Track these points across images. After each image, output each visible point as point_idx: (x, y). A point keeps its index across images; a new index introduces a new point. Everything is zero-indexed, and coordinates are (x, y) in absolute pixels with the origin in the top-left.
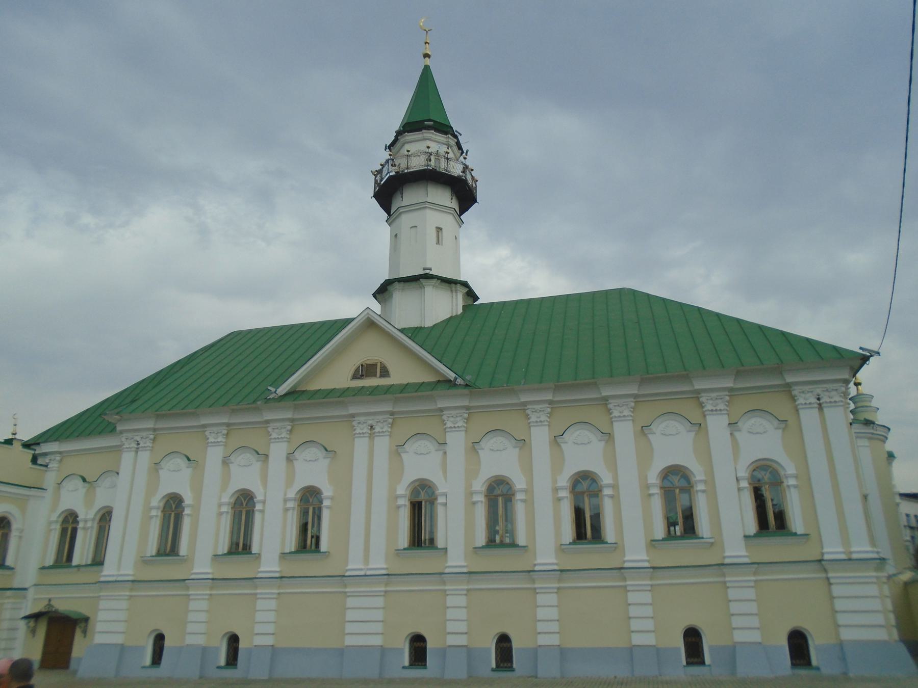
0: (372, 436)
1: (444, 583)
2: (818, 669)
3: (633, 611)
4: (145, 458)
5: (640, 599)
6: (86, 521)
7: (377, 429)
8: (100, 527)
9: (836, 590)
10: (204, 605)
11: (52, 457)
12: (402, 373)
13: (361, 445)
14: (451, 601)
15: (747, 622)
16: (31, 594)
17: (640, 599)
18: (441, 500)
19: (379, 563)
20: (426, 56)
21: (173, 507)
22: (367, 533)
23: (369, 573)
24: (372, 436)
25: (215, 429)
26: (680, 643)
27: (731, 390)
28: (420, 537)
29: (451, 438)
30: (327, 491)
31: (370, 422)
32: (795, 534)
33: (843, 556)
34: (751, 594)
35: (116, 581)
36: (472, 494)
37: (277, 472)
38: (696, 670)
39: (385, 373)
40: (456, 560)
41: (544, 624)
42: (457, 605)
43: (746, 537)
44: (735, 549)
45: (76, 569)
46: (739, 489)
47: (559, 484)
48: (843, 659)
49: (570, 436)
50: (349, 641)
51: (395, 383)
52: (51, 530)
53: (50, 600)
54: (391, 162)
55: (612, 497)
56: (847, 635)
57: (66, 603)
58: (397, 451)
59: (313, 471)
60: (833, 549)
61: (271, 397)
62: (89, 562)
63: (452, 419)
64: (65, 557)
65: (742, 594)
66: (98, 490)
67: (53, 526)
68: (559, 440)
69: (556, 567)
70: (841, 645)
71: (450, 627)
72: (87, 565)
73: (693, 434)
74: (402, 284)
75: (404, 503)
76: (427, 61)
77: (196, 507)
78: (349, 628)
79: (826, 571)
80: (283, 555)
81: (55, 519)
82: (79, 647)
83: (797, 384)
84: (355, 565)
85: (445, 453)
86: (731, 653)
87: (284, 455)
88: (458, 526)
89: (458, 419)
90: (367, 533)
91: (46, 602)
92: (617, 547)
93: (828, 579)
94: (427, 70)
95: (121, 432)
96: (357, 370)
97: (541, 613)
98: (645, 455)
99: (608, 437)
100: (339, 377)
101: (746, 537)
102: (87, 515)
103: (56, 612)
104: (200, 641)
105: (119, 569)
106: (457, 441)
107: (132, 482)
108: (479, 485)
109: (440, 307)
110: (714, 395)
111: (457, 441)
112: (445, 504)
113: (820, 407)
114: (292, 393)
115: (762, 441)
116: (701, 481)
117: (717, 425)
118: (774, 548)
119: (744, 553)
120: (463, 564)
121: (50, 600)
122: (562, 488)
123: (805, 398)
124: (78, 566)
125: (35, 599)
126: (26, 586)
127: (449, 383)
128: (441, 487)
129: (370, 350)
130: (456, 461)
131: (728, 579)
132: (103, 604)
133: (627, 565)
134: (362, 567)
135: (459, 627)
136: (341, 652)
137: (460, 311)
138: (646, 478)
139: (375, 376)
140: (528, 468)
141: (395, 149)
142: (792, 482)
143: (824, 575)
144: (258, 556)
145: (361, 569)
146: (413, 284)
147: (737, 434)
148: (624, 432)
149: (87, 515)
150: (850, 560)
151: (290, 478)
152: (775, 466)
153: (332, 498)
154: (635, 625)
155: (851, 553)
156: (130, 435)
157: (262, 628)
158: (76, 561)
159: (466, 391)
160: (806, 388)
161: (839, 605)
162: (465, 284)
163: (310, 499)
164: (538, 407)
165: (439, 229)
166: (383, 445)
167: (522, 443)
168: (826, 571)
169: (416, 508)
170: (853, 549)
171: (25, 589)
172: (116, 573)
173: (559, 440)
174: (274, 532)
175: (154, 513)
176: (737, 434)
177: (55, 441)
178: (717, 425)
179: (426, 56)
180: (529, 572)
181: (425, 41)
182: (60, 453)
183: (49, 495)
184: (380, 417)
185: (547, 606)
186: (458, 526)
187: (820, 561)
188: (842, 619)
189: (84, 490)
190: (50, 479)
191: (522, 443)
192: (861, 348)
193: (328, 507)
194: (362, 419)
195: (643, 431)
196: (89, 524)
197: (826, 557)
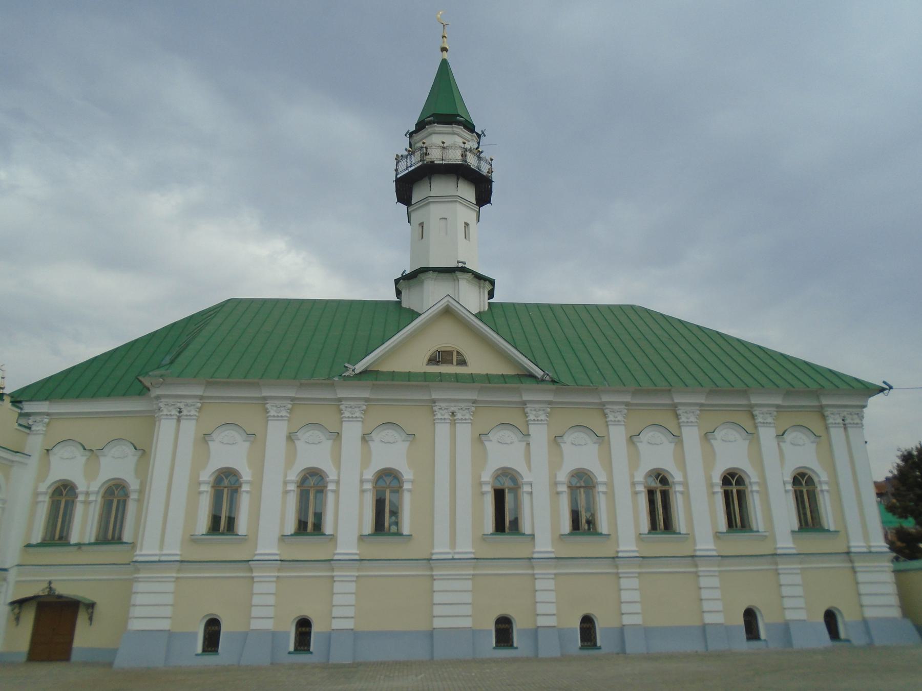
0: (453, 423)
1: (533, 568)
2: (848, 641)
3: (705, 594)
4: (189, 428)
5: (710, 582)
6: (87, 494)
7: (459, 416)
8: (53, 502)
9: (861, 577)
10: (272, 588)
11: (38, 418)
12: (480, 363)
13: (442, 431)
14: (539, 584)
15: (794, 603)
16: (12, 576)
17: (710, 582)
18: (526, 488)
19: (466, 547)
20: (444, 49)
21: (226, 484)
22: (450, 517)
23: (456, 556)
24: (453, 423)
25: (278, 403)
26: (741, 621)
27: (778, 406)
28: (505, 522)
29: (532, 429)
30: (407, 474)
31: (452, 409)
32: (828, 531)
33: (865, 550)
34: (798, 579)
35: (160, 561)
36: (556, 484)
37: (352, 452)
38: (754, 644)
39: (462, 361)
40: (544, 545)
41: (629, 605)
42: (546, 587)
43: (793, 532)
44: (705, 544)
45: (76, 548)
47: (636, 479)
48: (868, 632)
49: (646, 436)
50: (438, 623)
51: (474, 372)
52: (37, 503)
53: (50, 583)
54: (424, 150)
55: (682, 493)
56: (869, 613)
57: (68, 585)
58: (480, 438)
59: (391, 453)
60: (857, 544)
61: (346, 374)
62: (93, 540)
63: (534, 412)
64: (57, 536)
65: (792, 579)
66: (103, 460)
67: (41, 498)
68: (635, 439)
69: (637, 554)
70: (865, 621)
71: (540, 609)
72: (90, 544)
73: (747, 442)
74: (436, 274)
75: (488, 489)
76: (445, 55)
77: (258, 483)
78: (437, 611)
79: (851, 561)
80: (362, 538)
81: (44, 490)
82: (85, 637)
83: (828, 406)
84: (441, 548)
85: (528, 444)
86: (786, 629)
87: (360, 435)
88: (544, 515)
89: (541, 412)
90: (450, 517)
91: (46, 585)
92: (689, 537)
93: (853, 568)
94: (444, 63)
95: (158, 398)
97: (625, 596)
98: (709, 457)
99: (677, 439)
100: (414, 360)
101: (793, 532)
102: (90, 487)
103: (60, 597)
104: (268, 625)
105: (161, 547)
106: (540, 434)
107: (177, 453)
110: (765, 410)
111: (540, 434)
112: (531, 493)
113: (845, 427)
114: (365, 372)
115: (801, 453)
116: (756, 483)
117: (767, 435)
118: (813, 543)
119: (792, 545)
120: (550, 549)
121: (50, 583)
122: (639, 483)
123: (834, 419)
124: (79, 545)
125: (17, 582)
126: (6, 567)
127: (531, 376)
128: (527, 477)
129: (447, 337)
130: (542, 453)
131: (780, 567)
132: (140, 587)
133: (698, 553)
134: (448, 550)
135: (548, 608)
136: (431, 634)
138: (711, 477)
139: (452, 363)
141: (416, 137)
142: (825, 487)
143: (850, 565)
144: (333, 538)
145: (448, 553)
146: (447, 275)
147: (782, 444)
148: (618, 435)
149: (90, 487)
150: (870, 552)
151: (366, 459)
152: (810, 473)
153: (412, 482)
154: (706, 606)
155: (870, 547)
156: (171, 401)
157: (341, 610)
158: (74, 539)
160: (835, 410)
161: (863, 589)
163: (388, 480)
164: (616, 407)
165: (467, 224)
166: (465, 432)
167: (602, 440)
168: (851, 561)
169: (499, 496)
170: (872, 544)
171: (5, 570)
172: (158, 552)
173: (635, 439)
174: (348, 514)
175: (204, 488)
176: (782, 444)
177: (46, 399)
178: (767, 435)
179: (444, 49)
180: (613, 558)
181: (442, 34)
182: (48, 414)
183: (34, 463)
184: (463, 405)
185: (631, 589)
186: (544, 515)
187: (848, 553)
188: (865, 601)
189: (84, 459)
190: (35, 443)
191: (602, 440)
192: (884, 382)
193: (409, 491)
194: (444, 405)
195: (707, 436)
196: (92, 498)
197: (853, 550)
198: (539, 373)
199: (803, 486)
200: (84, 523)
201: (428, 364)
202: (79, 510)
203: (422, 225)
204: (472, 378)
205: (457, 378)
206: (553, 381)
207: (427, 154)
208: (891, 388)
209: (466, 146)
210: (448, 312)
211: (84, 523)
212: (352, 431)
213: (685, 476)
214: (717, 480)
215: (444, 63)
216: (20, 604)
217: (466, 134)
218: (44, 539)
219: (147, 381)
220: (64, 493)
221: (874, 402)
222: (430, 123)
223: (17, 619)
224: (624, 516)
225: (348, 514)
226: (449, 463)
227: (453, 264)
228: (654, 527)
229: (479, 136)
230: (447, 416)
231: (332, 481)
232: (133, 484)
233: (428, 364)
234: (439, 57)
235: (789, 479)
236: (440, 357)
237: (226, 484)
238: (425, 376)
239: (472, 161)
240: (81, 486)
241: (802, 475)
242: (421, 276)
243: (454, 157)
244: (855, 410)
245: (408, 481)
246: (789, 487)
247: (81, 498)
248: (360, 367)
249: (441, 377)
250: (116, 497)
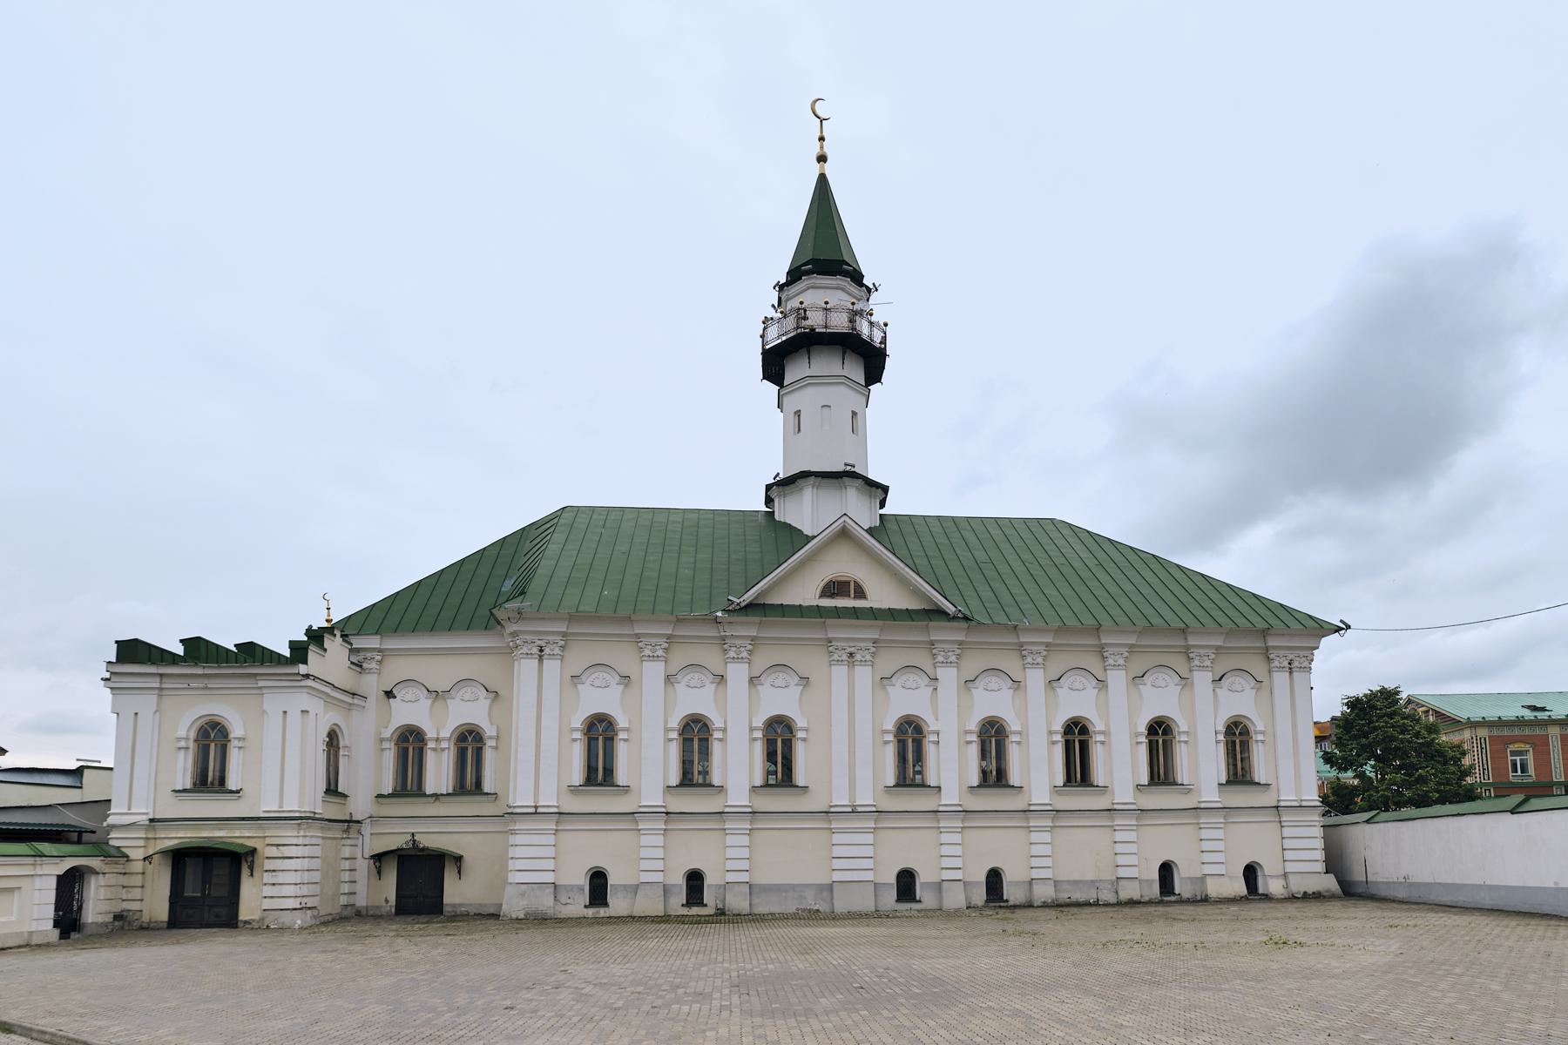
6: (437, 740)
12: (882, 594)
16: (367, 829)
29: (942, 673)
39: (860, 593)
51: (875, 605)
57: (433, 838)
64: (409, 784)
67: (386, 745)
88: (952, 764)
91: (409, 837)
94: (822, 181)
100: (806, 592)
103: (424, 849)
115: (1239, 701)
117: (1202, 679)
124: (436, 796)
127: (937, 613)
128: (931, 724)
129: (843, 565)
159: (964, 625)
174: (738, 763)
198: (951, 609)
199: (1237, 737)
200: (439, 772)
201: (821, 596)
202: (430, 759)
203: (798, 413)
204: (874, 614)
205: (855, 613)
206: (966, 618)
207: (805, 318)
208: (1349, 627)
209: (856, 307)
210: (844, 534)
211: (439, 772)
212: (737, 674)
213: (1107, 725)
214: (1143, 729)
216: (379, 858)
217: (854, 289)
218: (395, 790)
219: (500, 614)
220: (410, 743)
221: (1328, 642)
222: (808, 273)
223: (379, 873)
224: (1037, 765)
225: (738, 763)
226: (846, 711)
227: (840, 468)
228: (1069, 780)
229: (869, 290)
230: (844, 657)
231: (719, 729)
232: (489, 730)
233: (821, 596)
234: (814, 170)
235: (1221, 728)
236: (835, 588)
237: (600, 732)
238: (818, 612)
239: (864, 329)
240: (430, 733)
241: (1236, 724)
242: (800, 482)
243: (839, 323)
244: (1302, 653)
245: (802, 729)
246: (1221, 737)
247: (431, 745)
248: (748, 597)
249: (838, 613)
250: (469, 742)
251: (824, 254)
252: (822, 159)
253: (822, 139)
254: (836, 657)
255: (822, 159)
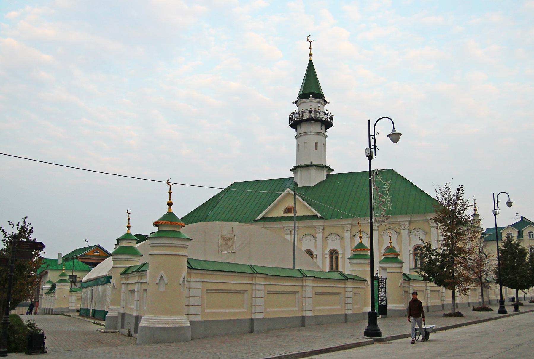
46: (410, 254)
74: (301, 168)
94: (311, 63)
96: (285, 210)
100: (279, 213)
108: (327, 252)
109: (315, 178)
127: (317, 216)
137: (325, 178)
140: (343, 247)
147: (411, 236)
162: (327, 167)
191: (341, 238)
198: (319, 215)
215: (311, 63)
227: (309, 163)
230: (289, 232)
236: (288, 210)
246: (411, 252)
251: (311, 89)
252: (310, 55)
253: (310, 48)
254: (286, 232)
255: (310, 55)
